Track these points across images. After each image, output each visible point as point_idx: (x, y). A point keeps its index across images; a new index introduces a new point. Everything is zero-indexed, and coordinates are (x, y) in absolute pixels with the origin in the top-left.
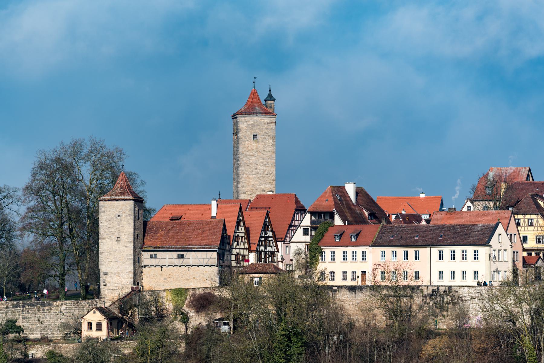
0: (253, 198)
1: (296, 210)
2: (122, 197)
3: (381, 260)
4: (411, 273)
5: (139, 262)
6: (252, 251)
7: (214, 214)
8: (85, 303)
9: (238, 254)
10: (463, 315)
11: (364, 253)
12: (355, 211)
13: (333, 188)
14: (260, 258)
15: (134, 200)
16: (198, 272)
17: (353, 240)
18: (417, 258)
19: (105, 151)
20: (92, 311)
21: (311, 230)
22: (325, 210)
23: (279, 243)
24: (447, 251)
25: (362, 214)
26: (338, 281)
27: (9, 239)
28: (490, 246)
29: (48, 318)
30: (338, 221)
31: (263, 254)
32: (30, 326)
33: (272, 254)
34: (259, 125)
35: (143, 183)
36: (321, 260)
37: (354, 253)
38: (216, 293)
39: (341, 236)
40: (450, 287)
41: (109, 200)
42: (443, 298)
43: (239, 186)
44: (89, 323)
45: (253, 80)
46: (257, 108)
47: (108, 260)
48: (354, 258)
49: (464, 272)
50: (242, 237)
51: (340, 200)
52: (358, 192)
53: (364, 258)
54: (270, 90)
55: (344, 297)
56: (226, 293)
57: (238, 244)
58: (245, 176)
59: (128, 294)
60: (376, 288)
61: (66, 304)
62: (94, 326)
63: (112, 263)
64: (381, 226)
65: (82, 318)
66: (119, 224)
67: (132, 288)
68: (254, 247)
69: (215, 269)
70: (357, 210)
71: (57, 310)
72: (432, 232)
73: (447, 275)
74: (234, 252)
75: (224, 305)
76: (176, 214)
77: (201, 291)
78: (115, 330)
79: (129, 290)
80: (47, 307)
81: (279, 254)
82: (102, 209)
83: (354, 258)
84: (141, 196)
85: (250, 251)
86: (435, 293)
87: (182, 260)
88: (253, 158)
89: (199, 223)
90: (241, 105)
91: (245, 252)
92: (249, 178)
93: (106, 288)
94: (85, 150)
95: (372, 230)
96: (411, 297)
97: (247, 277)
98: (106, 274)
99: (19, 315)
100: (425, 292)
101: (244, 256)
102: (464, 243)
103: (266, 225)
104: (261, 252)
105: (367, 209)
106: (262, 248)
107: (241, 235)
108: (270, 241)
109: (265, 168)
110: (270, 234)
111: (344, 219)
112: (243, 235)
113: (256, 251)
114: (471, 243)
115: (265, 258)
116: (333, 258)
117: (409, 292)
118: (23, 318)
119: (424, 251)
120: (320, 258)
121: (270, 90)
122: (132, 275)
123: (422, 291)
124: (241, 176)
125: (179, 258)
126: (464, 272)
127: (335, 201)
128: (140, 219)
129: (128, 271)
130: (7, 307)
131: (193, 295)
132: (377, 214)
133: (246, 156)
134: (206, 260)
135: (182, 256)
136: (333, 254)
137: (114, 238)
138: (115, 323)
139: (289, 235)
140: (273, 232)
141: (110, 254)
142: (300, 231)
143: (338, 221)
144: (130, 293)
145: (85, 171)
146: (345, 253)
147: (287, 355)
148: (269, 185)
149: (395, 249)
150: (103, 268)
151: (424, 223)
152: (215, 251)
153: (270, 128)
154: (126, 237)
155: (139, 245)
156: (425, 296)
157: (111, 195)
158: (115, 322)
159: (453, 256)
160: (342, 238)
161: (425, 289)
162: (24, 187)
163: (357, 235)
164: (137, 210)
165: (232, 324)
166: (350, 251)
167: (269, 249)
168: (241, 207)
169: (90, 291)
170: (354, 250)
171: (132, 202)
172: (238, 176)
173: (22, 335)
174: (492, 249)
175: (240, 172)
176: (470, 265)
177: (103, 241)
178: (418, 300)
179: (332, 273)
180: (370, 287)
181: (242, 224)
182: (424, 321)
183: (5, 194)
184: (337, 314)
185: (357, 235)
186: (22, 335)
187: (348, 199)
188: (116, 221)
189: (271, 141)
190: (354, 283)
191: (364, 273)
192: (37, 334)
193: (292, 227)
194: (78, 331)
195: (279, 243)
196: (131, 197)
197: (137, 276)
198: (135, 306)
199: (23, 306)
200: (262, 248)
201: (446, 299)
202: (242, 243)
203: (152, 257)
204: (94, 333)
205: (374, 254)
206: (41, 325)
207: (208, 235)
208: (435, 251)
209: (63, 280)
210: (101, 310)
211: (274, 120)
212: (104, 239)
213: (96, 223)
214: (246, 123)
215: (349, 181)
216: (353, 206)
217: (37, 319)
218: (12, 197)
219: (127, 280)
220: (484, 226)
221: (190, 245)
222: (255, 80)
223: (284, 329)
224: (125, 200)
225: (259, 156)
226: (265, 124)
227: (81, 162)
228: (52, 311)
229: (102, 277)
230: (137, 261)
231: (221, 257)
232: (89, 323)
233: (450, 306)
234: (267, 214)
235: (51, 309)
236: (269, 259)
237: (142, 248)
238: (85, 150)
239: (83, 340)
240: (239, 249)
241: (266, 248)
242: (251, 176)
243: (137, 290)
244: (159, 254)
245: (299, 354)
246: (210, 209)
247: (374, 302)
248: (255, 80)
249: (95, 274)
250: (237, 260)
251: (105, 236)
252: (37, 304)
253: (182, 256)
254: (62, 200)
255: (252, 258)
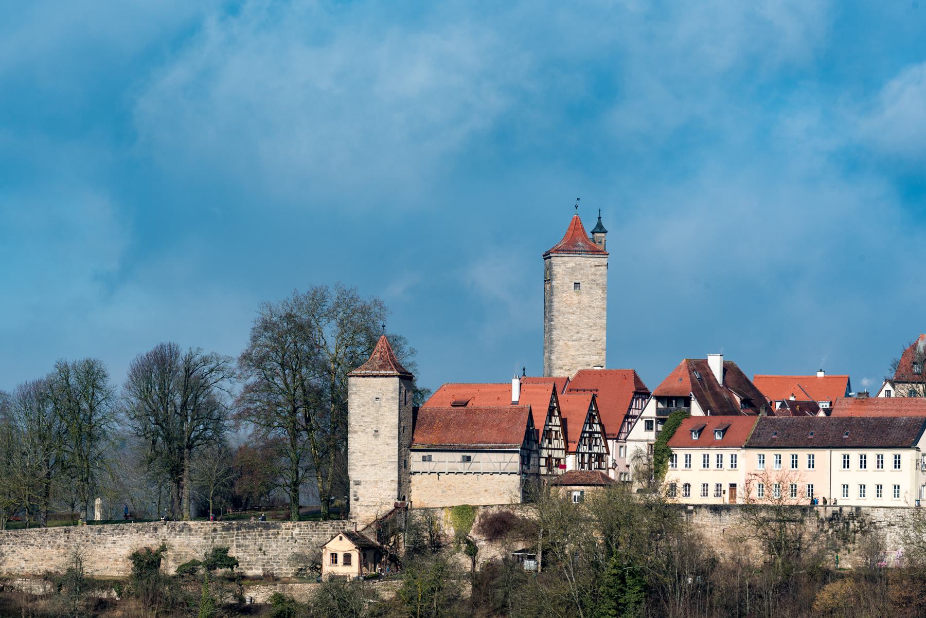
0: (572, 375)
1: (636, 393)
2: (383, 372)
3: (758, 468)
4: (802, 486)
5: (405, 467)
6: (571, 453)
7: (515, 397)
8: (328, 526)
9: (550, 456)
10: (876, 549)
11: (734, 459)
12: (722, 397)
13: (689, 362)
14: (582, 464)
15: (399, 376)
16: (492, 482)
17: (718, 437)
18: (811, 465)
19: (358, 305)
20: (338, 538)
21: (657, 423)
22: (678, 394)
23: (610, 442)
24: (855, 455)
25: (732, 401)
26: (695, 498)
27: (218, 430)
28: (918, 449)
29: (274, 546)
30: (696, 410)
31: (586, 456)
32: (248, 558)
33: (600, 457)
34: (582, 269)
35: (413, 352)
36: (670, 467)
37: (720, 458)
38: (518, 513)
39: (700, 431)
40: (858, 508)
41: (363, 376)
42: (848, 524)
43: (553, 357)
44: (332, 554)
45: (575, 202)
46: (580, 243)
47: (361, 464)
48: (719, 464)
49: (879, 487)
50: (556, 432)
51: (700, 379)
52: (727, 369)
53: (734, 464)
54: (600, 218)
55: (703, 520)
56: (532, 514)
57: (550, 443)
58: (561, 343)
59: (390, 513)
60: (750, 508)
61: (299, 526)
62: (340, 559)
63: (367, 468)
64: (758, 418)
65: (323, 546)
66: (378, 411)
67: (396, 504)
68: (573, 447)
69: (517, 479)
70: (725, 394)
71: (287, 534)
72: (834, 428)
73: (854, 490)
74: (545, 453)
75: (528, 530)
76: (461, 397)
77: (495, 510)
78: (371, 566)
79: (391, 507)
80: (272, 531)
81: (610, 458)
82: (352, 389)
83: (719, 464)
84: (410, 370)
85: (567, 452)
86: (836, 517)
87: (468, 464)
88: (574, 317)
89: (493, 411)
90: (559, 240)
91: (561, 454)
92: (568, 346)
93: (358, 503)
94: (330, 303)
95: (746, 424)
96: (802, 521)
97: (562, 490)
98: (358, 483)
99: (233, 541)
100: (822, 515)
101: (558, 460)
102: (879, 444)
103: (591, 415)
104: (583, 454)
105: (739, 394)
106: (584, 449)
107: (554, 428)
108: (596, 439)
109: (591, 332)
110: (597, 428)
111: (705, 406)
112: (557, 429)
113: (576, 453)
114: (891, 444)
115: (590, 463)
116: (688, 464)
117: (799, 514)
118: (238, 546)
119: (821, 455)
120: (670, 463)
121: (600, 218)
122: (396, 486)
123: (817, 514)
124: (555, 343)
125: (463, 461)
126: (879, 487)
127: (692, 380)
128: (408, 404)
129: (389, 479)
130: (215, 530)
131: (484, 516)
132: (754, 401)
133: (564, 314)
134: (503, 465)
135: (468, 459)
136: (688, 458)
137: (370, 431)
138: (370, 554)
139: (625, 430)
140: (602, 426)
141: (365, 454)
142: (641, 424)
143: (696, 410)
144: (393, 511)
145: (329, 334)
146: (706, 458)
147: (619, 604)
148: (597, 357)
149: (778, 452)
150: (353, 475)
151: (821, 414)
152: (517, 452)
153: (599, 273)
154: (388, 429)
155: (406, 442)
156: (822, 521)
157: (366, 369)
158: (371, 552)
159: (863, 464)
160: (702, 436)
161: (821, 510)
162: (240, 355)
163: (724, 431)
164: (403, 390)
165: (539, 559)
166: (713, 453)
167: (596, 449)
168: (554, 389)
169: (335, 507)
170: (720, 452)
171: (397, 379)
172: (551, 343)
173: (236, 570)
174: (920, 453)
175: (554, 337)
176: (888, 476)
177: (355, 436)
178: (811, 526)
179: (687, 486)
180: (744, 508)
181: (556, 414)
182: (820, 556)
183: (212, 366)
184: (692, 546)
185: (724, 431)
186: (236, 570)
187: (712, 378)
188: (373, 406)
189: (600, 292)
190: (718, 501)
191: (733, 486)
192: (257, 569)
193: (628, 417)
194: (316, 565)
195: (610, 442)
196: (396, 372)
197: (403, 488)
198: (400, 530)
199: (238, 529)
200: (584, 449)
201: (852, 526)
202: (556, 441)
203: (424, 459)
204: (340, 569)
205: (748, 459)
206: (264, 557)
207: (506, 429)
208: (838, 454)
209: (296, 491)
210: (350, 535)
211: (604, 261)
212: (356, 432)
213: (344, 409)
214: (563, 265)
215: (714, 353)
216: (718, 389)
217: (257, 547)
218: (222, 370)
219: (388, 492)
220: (910, 419)
221: (480, 443)
222: (579, 203)
223: (615, 566)
224: (386, 376)
225: (583, 314)
226: (591, 267)
227: (324, 320)
228: (280, 537)
229: (353, 489)
230: (403, 464)
231: (525, 460)
232: (332, 554)
233: (858, 535)
234: (593, 399)
235: (278, 534)
236: (595, 465)
237: (410, 446)
238: (330, 303)
239: (324, 578)
240: (552, 449)
241: (590, 449)
242: (570, 343)
243: (402, 507)
244: (435, 456)
245: (636, 603)
246: (510, 390)
247: (748, 528)
248: (579, 203)
249: (342, 484)
250: (549, 465)
251: (357, 428)
252: (258, 525)
253: (468, 459)
254: (294, 376)
255: (571, 463)
